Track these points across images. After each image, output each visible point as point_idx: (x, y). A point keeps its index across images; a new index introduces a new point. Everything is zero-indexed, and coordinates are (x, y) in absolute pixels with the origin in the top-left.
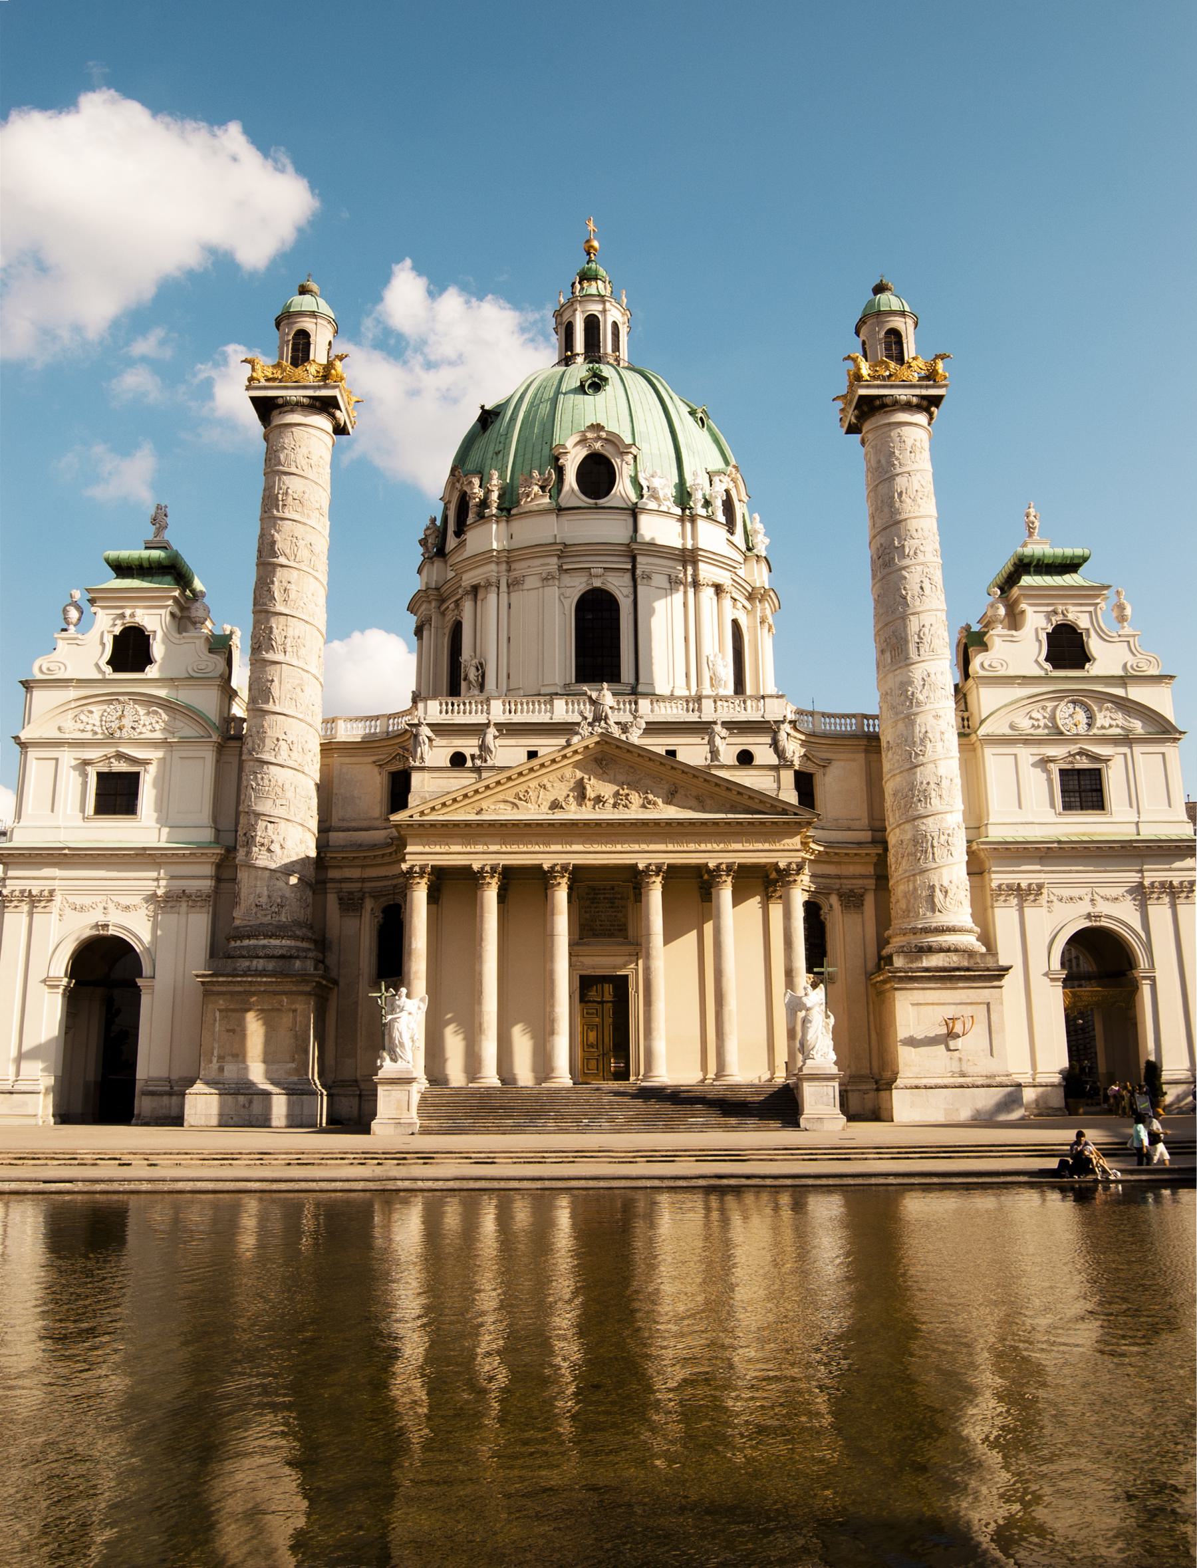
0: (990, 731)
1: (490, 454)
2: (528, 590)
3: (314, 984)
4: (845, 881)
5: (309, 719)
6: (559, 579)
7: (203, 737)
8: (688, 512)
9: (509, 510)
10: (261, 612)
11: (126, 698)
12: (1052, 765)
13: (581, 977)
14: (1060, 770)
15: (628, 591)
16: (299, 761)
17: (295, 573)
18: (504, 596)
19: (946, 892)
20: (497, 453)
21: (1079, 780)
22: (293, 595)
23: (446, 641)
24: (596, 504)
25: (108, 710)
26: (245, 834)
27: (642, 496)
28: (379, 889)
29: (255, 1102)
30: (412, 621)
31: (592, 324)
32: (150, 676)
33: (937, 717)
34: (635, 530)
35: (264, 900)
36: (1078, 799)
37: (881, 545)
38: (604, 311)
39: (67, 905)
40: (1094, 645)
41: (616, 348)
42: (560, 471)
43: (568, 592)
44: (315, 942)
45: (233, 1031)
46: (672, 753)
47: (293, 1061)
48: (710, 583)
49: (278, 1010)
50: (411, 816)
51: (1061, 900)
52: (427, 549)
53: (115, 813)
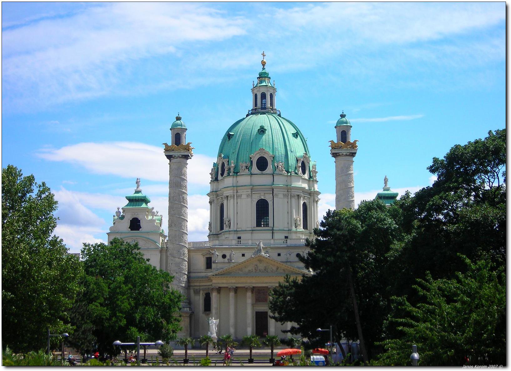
1: (231, 153)
3: (189, 314)
8: (289, 174)
9: (237, 173)
10: (171, 216)
13: (256, 312)
17: (180, 206)
18: (235, 200)
20: (233, 153)
23: (219, 208)
24: (262, 173)
30: (208, 199)
31: (263, 96)
32: (142, 231)
34: (274, 181)
37: (338, 195)
38: (268, 91)
41: (272, 104)
43: (254, 199)
44: (188, 303)
46: (279, 255)
47: (185, 333)
52: (212, 178)
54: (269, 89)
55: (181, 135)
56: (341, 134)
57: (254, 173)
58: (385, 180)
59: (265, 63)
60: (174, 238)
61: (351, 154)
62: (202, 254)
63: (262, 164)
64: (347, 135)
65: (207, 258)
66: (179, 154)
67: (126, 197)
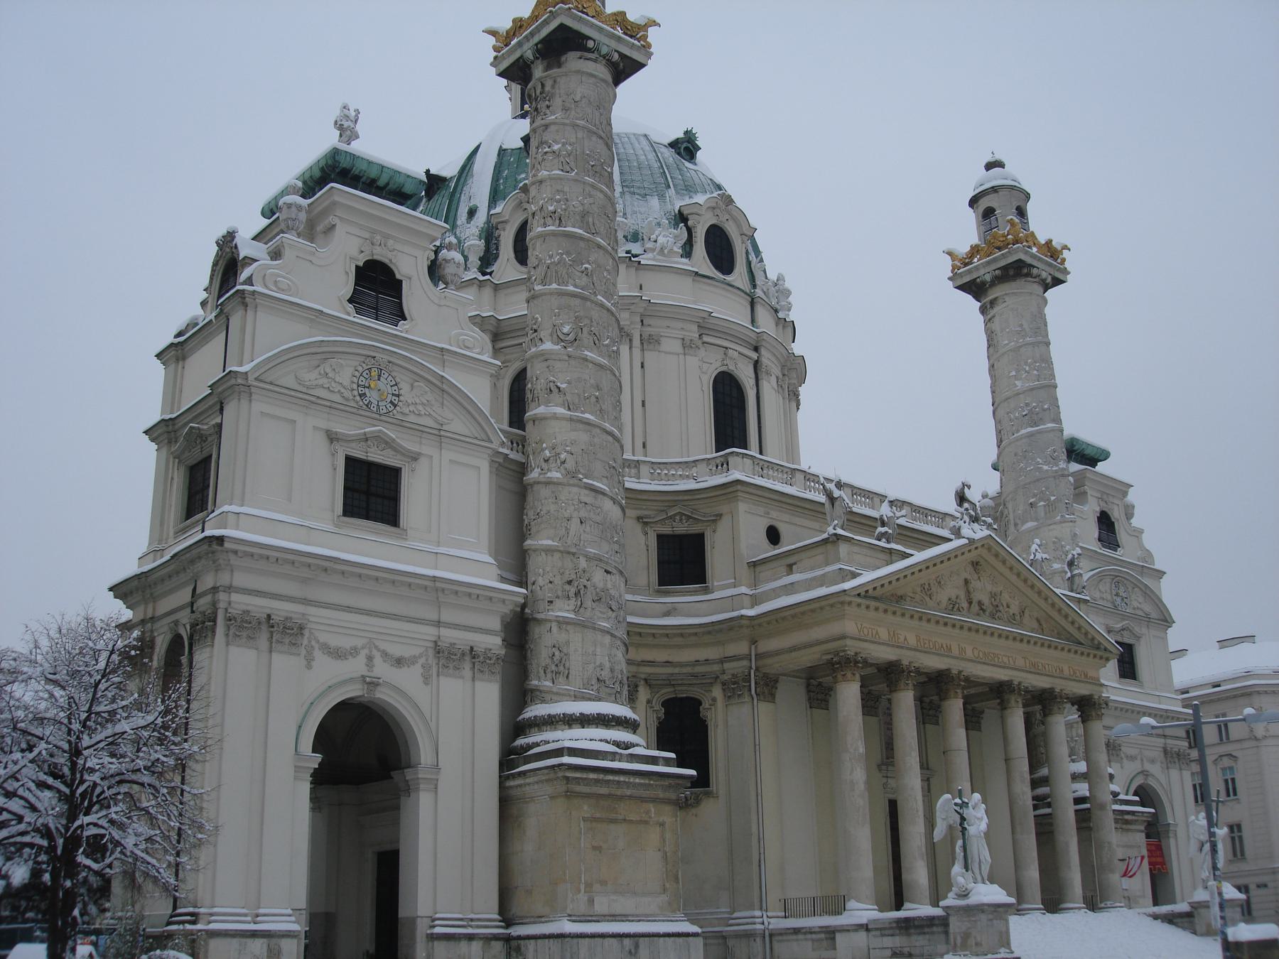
2: (666, 353)
7: (476, 438)
11: (387, 358)
15: (753, 382)
25: (360, 369)
26: (570, 582)
28: (664, 677)
29: (642, 946)
39: (316, 646)
40: (1122, 536)
42: (689, 231)
43: (705, 366)
45: (597, 848)
47: (665, 890)
49: (646, 822)
50: (859, 595)
53: (367, 518)
60: (593, 399)
62: (639, 518)
65: (660, 538)
66: (614, 44)
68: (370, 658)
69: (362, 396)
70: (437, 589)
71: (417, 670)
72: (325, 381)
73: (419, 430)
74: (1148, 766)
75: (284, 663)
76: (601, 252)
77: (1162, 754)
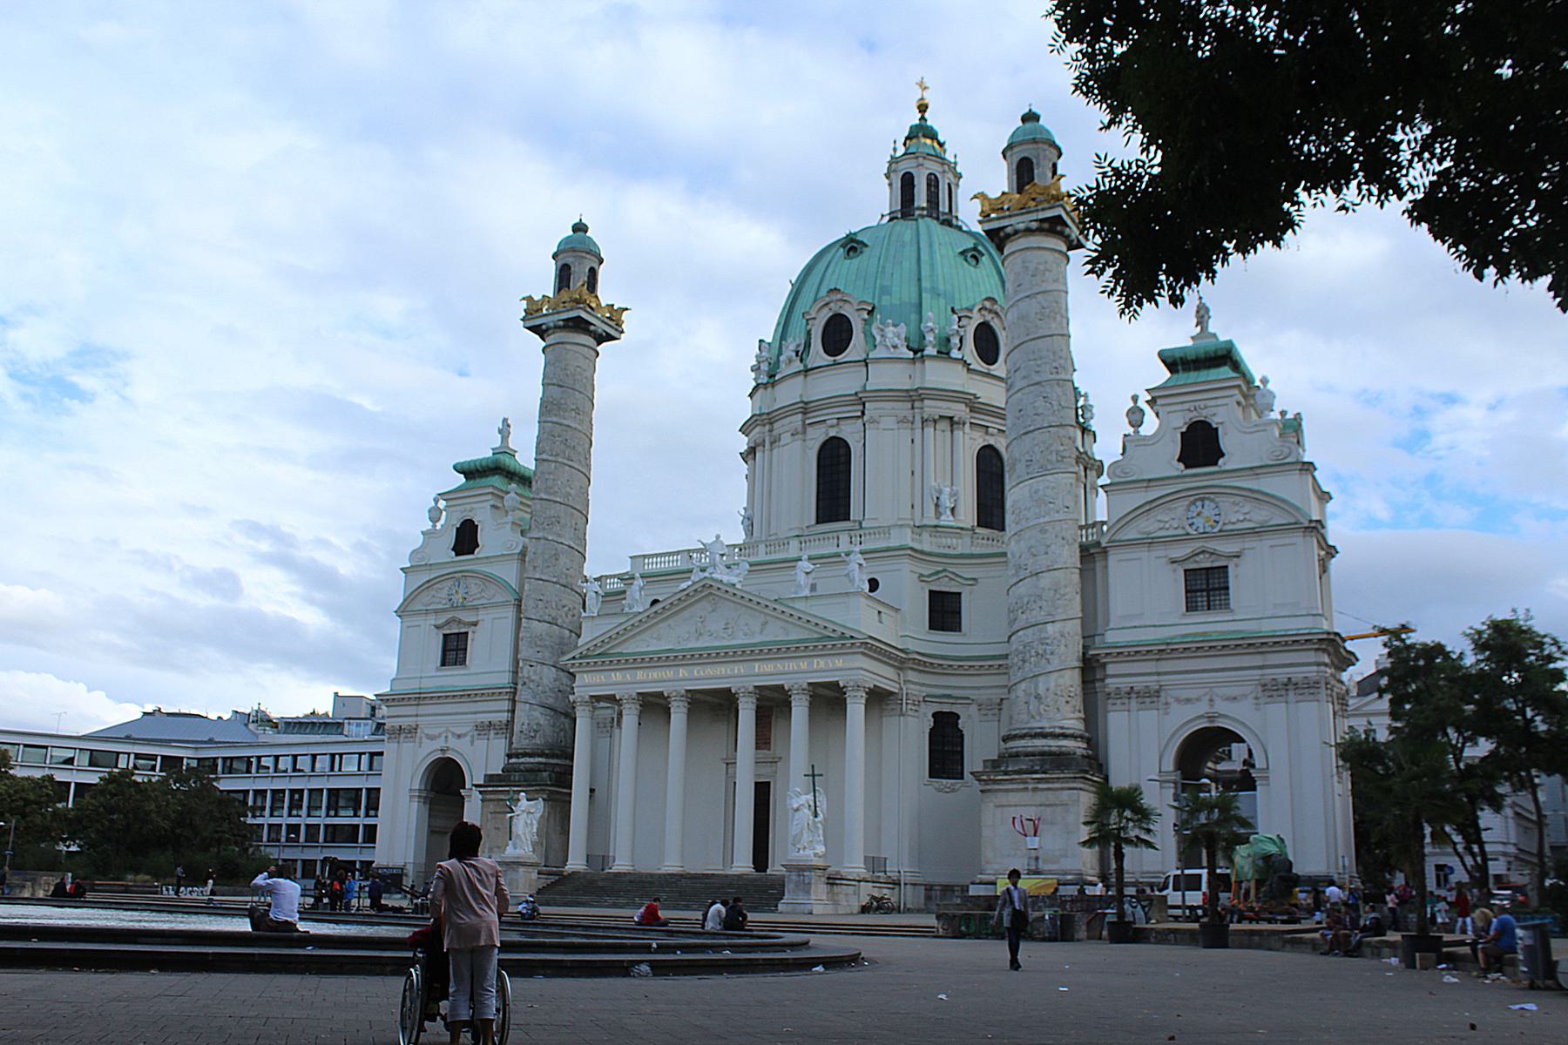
0: (1116, 537)
2: (783, 446)
4: (981, 691)
5: (561, 581)
6: (804, 432)
8: (919, 355)
9: (774, 376)
12: (1175, 565)
14: (1186, 571)
16: (554, 615)
17: (553, 465)
19: (1041, 698)
21: (1208, 580)
22: (550, 483)
27: (875, 346)
32: (480, 556)
33: (1044, 531)
35: (525, 727)
36: (1205, 599)
42: (809, 333)
43: (810, 443)
45: (498, 829)
48: (937, 417)
50: (574, 658)
51: (1178, 700)
53: (456, 664)
54: (921, 160)
55: (572, 269)
56: (1015, 172)
57: (814, 366)
58: (1198, 312)
59: (926, 107)
61: (1046, 226)
63: (837, 335)
64: (1036, 171)
66: (557, 317)
67: (455, 468)
68: (446, 737)
69: (450, 600)
70: (467, 695)
71: (468, 738)
72: (434, 600)
73: (476, 608)
74: (1221, 707)
75: (407, 746)
76: (546, 463)
77: (1260, 688)
